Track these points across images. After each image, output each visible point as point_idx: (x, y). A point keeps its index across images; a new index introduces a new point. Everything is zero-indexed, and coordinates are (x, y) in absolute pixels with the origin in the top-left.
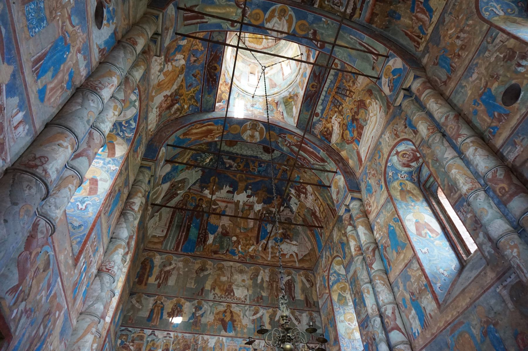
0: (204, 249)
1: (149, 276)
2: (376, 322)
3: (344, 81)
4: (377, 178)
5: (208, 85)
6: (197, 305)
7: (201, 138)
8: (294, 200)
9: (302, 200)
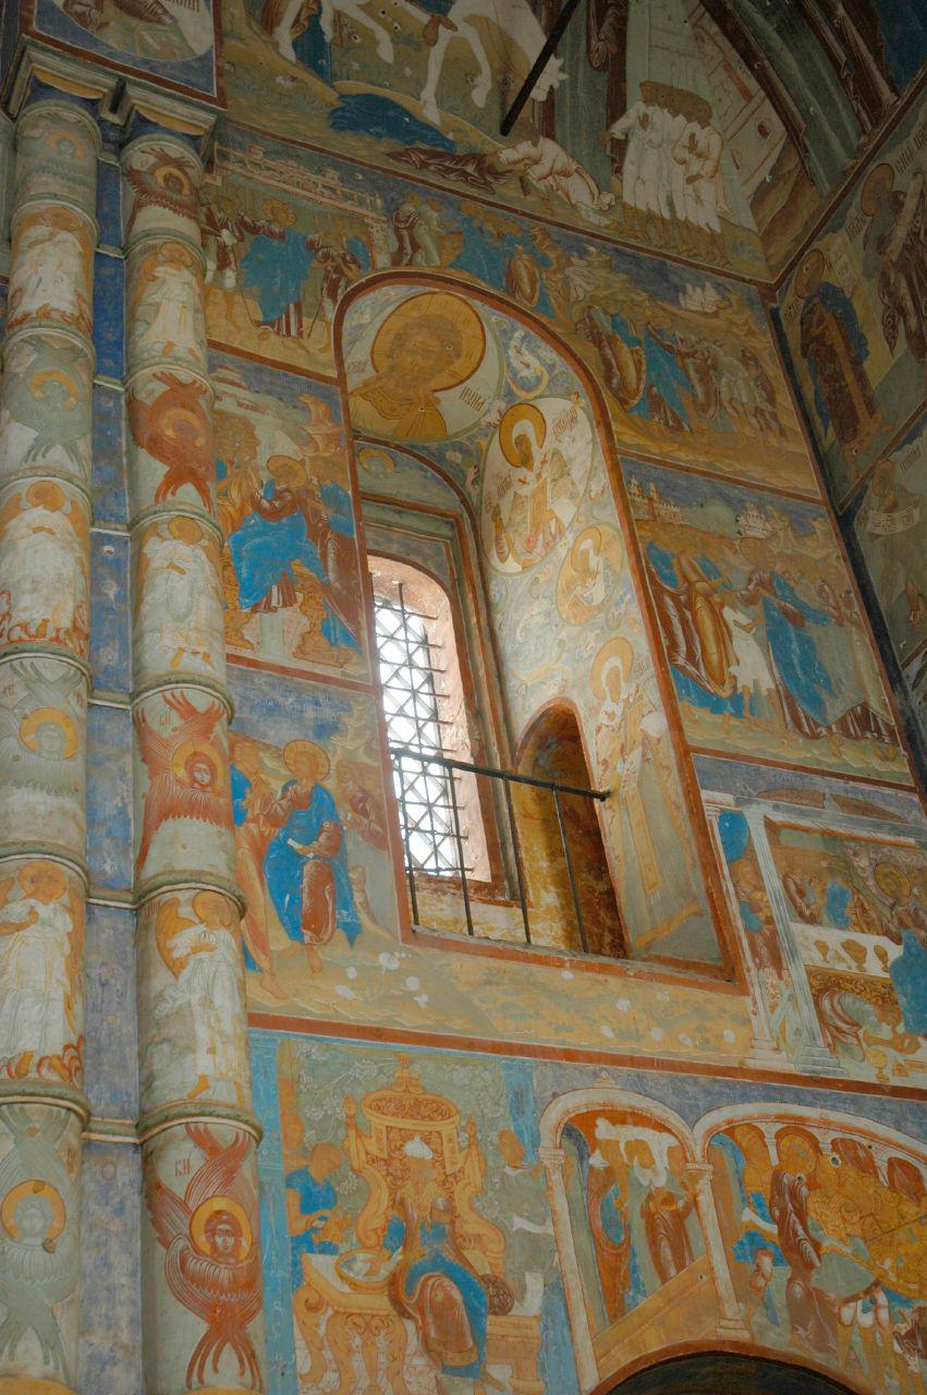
1: (857, 363)
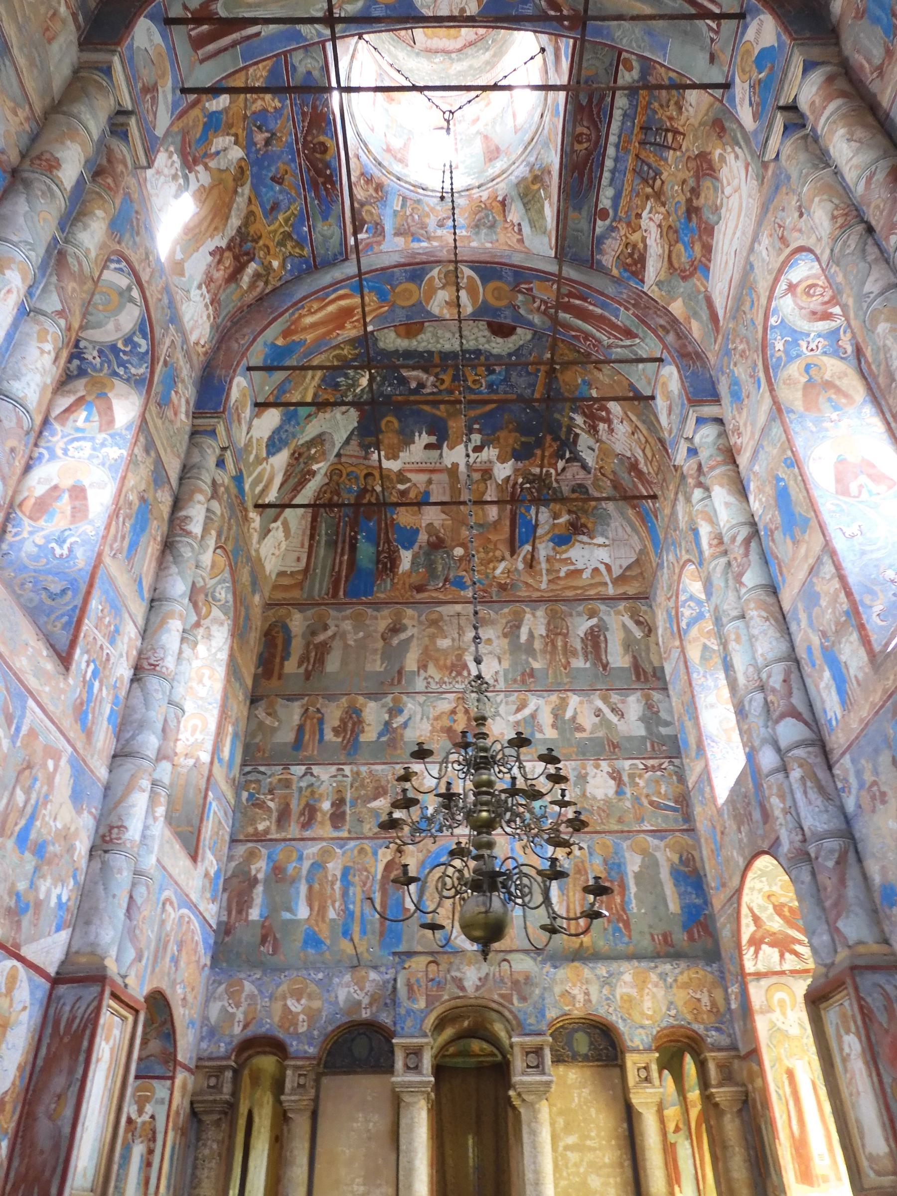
0: (393, 584)
2: (754, 704)
3: (656, 105)
4: (749, 361)
5: (318, 196)
6: (391, 705)
7: (330, 332)
8: (585, 441)
9: (604, 438)
